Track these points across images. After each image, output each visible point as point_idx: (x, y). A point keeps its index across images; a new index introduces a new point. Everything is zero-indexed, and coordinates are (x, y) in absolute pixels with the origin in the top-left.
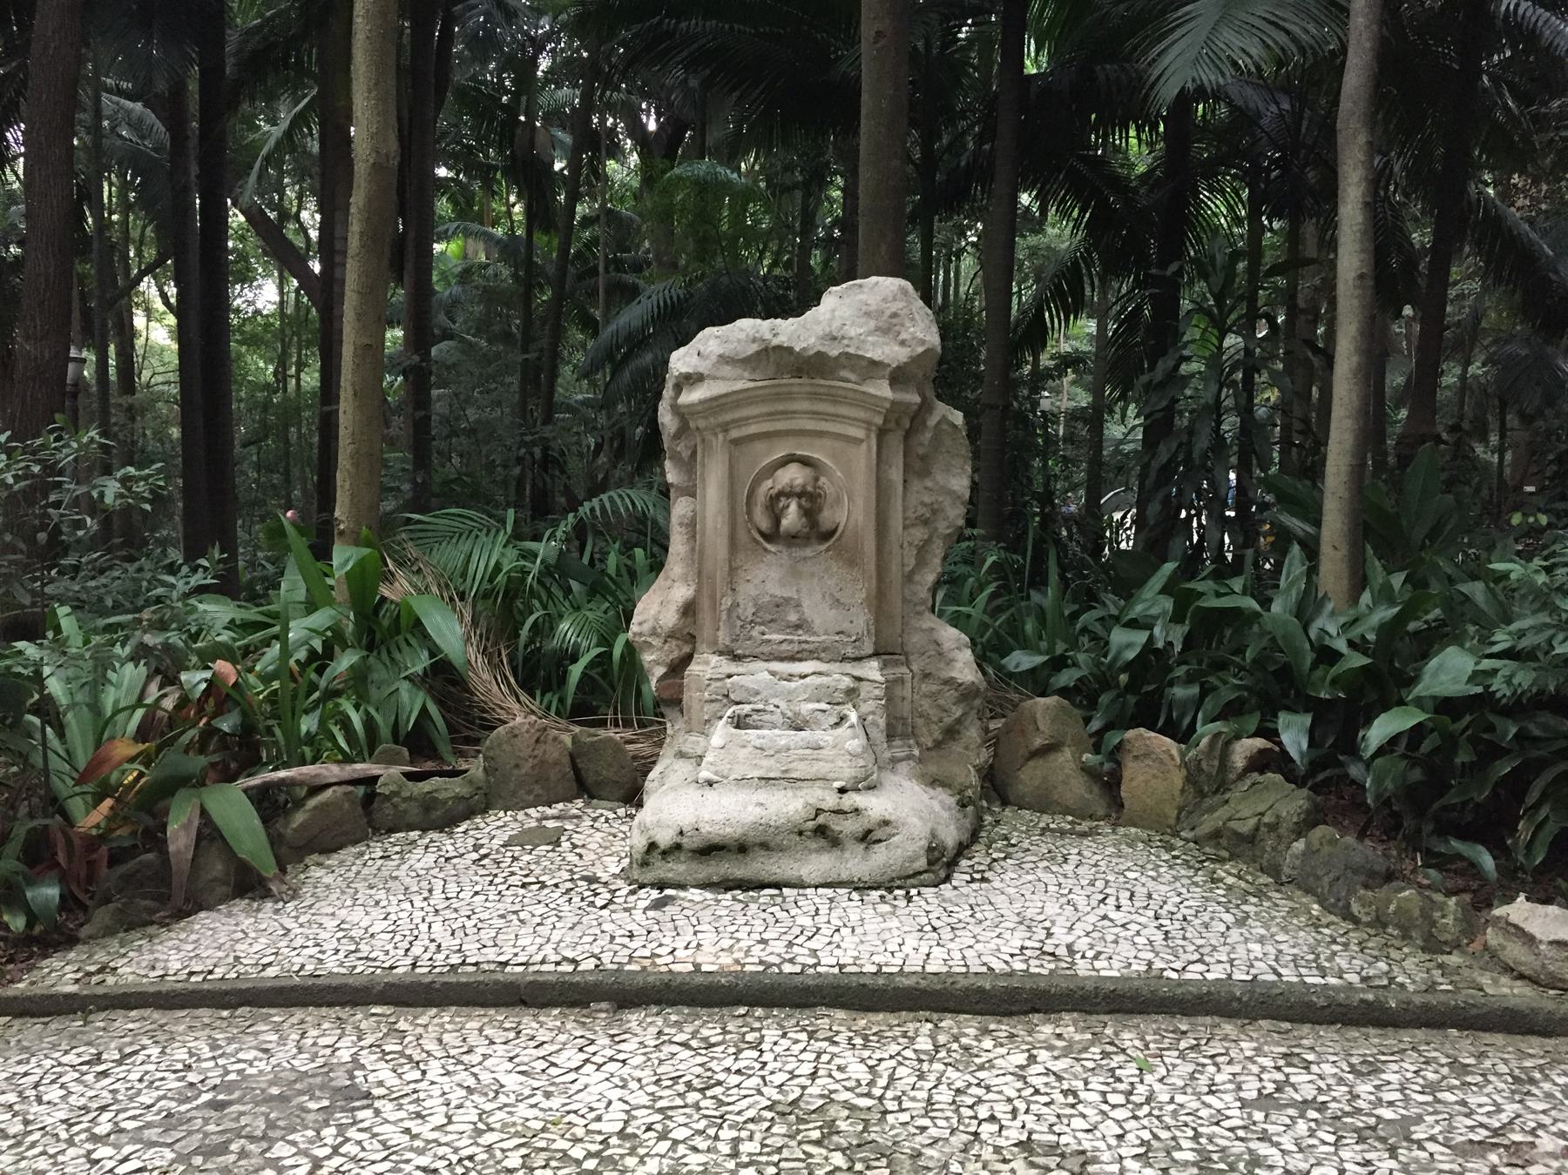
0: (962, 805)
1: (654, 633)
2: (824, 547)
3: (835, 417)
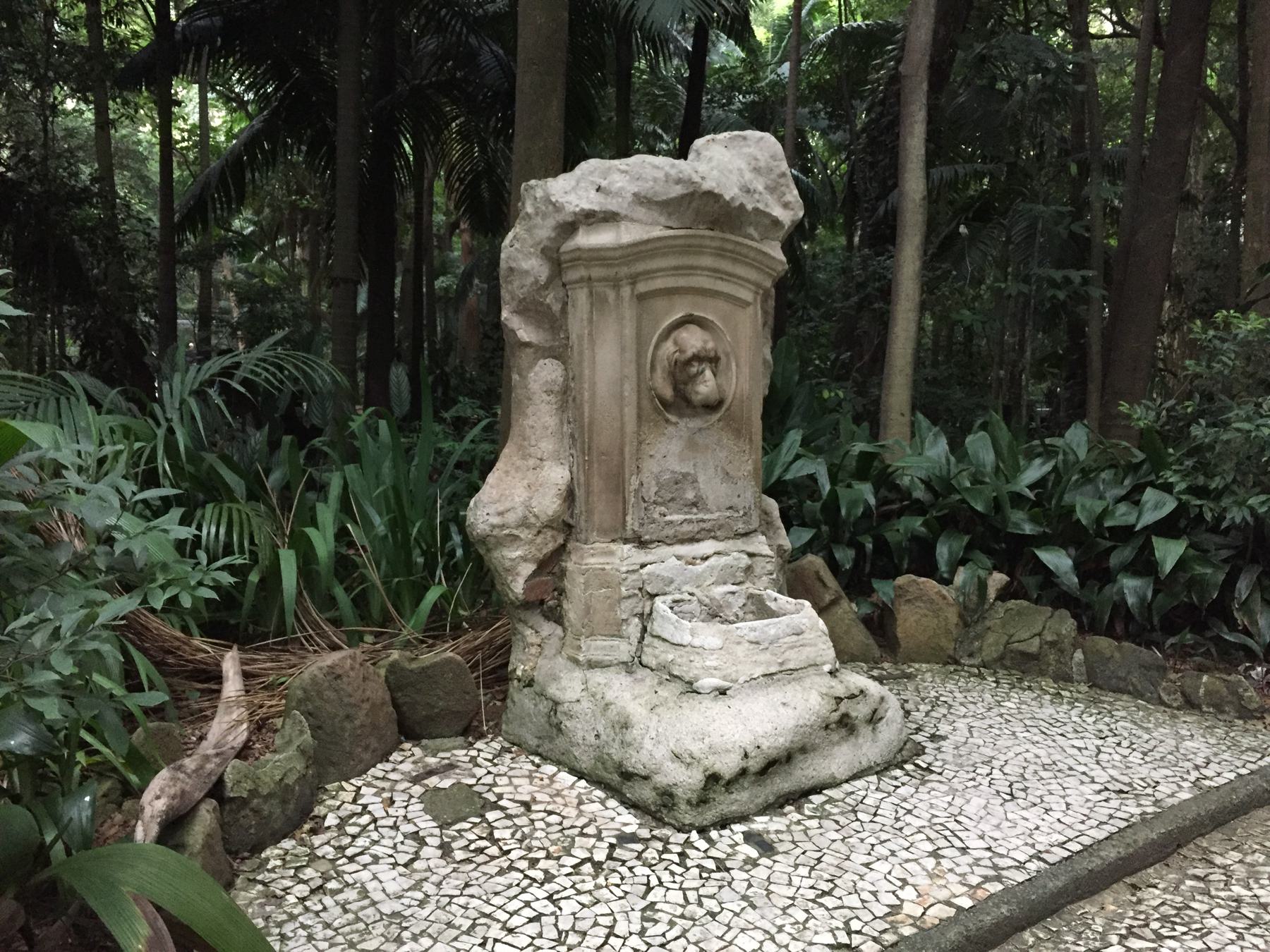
1: (524, 523)
2: (718, 415)
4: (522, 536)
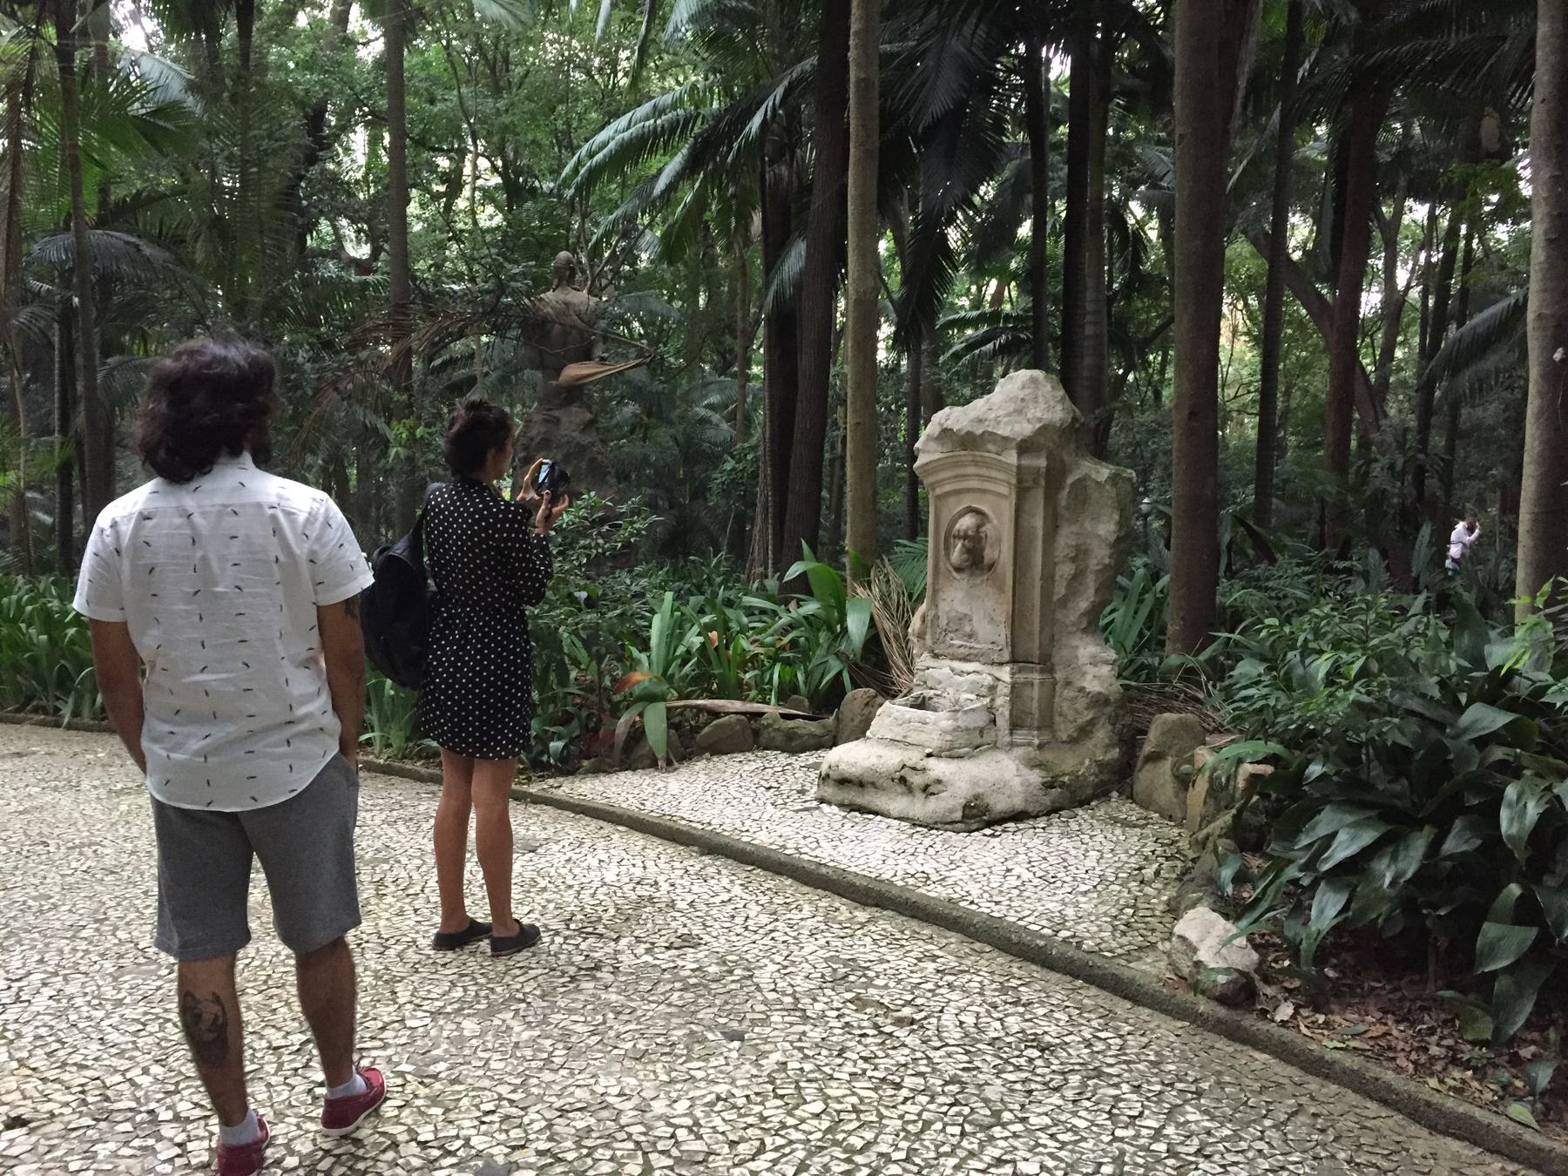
0: (1049, 786)
3: (989, 479)
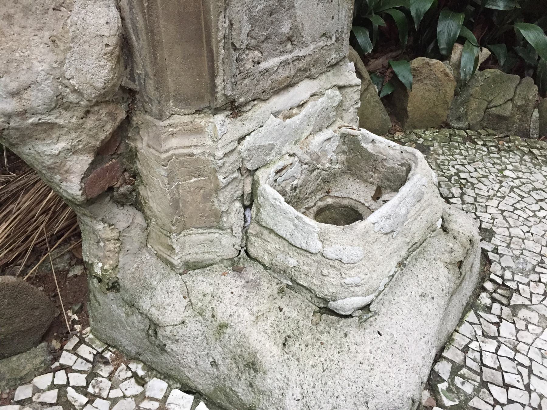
4: (61, 122)
